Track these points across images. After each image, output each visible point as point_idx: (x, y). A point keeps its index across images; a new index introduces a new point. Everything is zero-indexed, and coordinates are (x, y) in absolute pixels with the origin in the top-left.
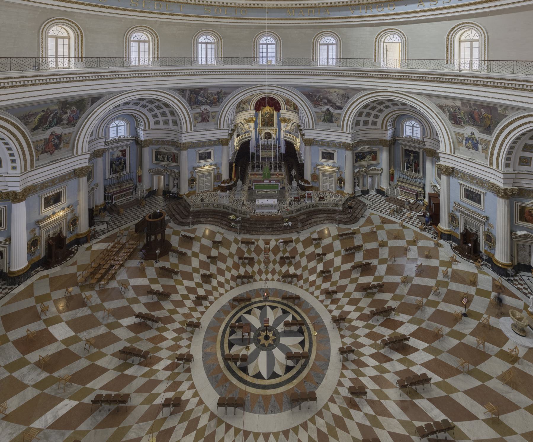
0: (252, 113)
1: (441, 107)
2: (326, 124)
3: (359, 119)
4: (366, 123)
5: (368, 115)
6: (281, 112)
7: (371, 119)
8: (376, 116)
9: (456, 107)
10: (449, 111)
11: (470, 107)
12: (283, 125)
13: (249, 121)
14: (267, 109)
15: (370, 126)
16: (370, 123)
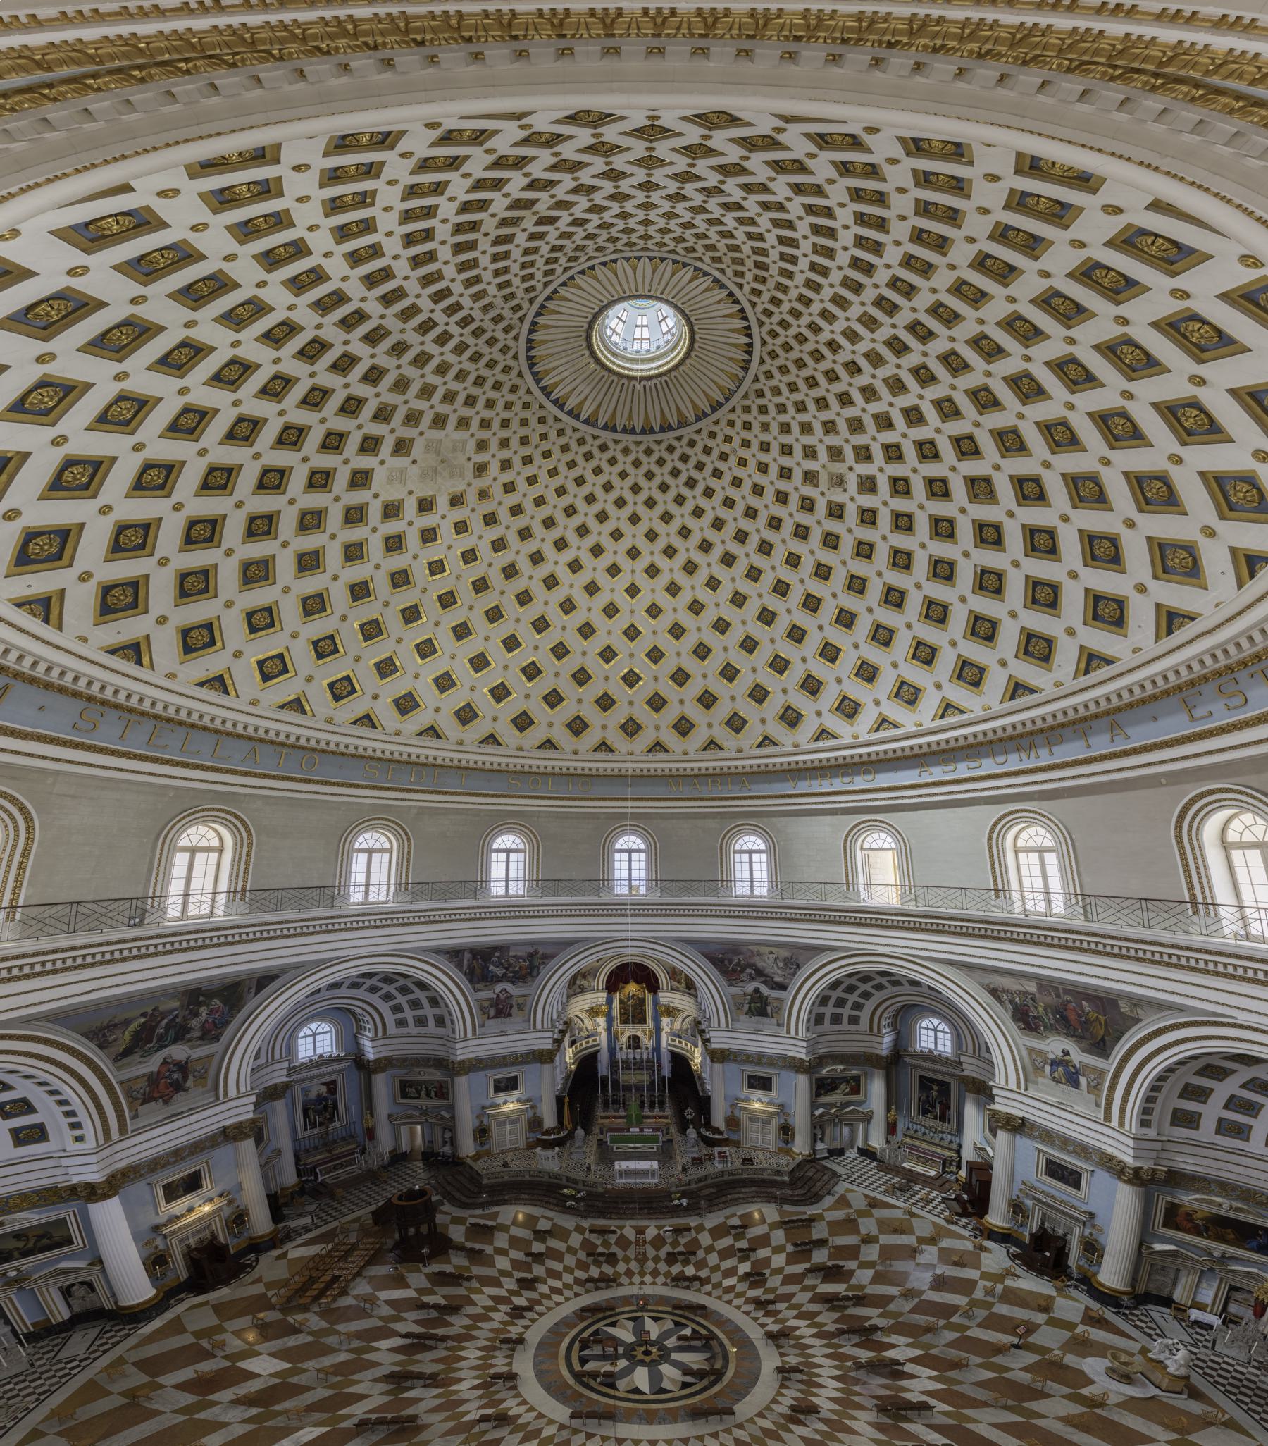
0: (600, 997)
1: (994, 992)
2: (754, 1019)
3: (822, 1010)
4: (836, 1019)
5: (841, 1003)
6: (660, 994)
7: (846, 1011)
8: (857, 1006)
9: (1026, 993)
10: (1011, 1001)
11: (1058, 996)
12: (665, 1021)
13: (594, 1012)
14: (632, 988)
15: (845, 1026)
16: (845, 1019)
